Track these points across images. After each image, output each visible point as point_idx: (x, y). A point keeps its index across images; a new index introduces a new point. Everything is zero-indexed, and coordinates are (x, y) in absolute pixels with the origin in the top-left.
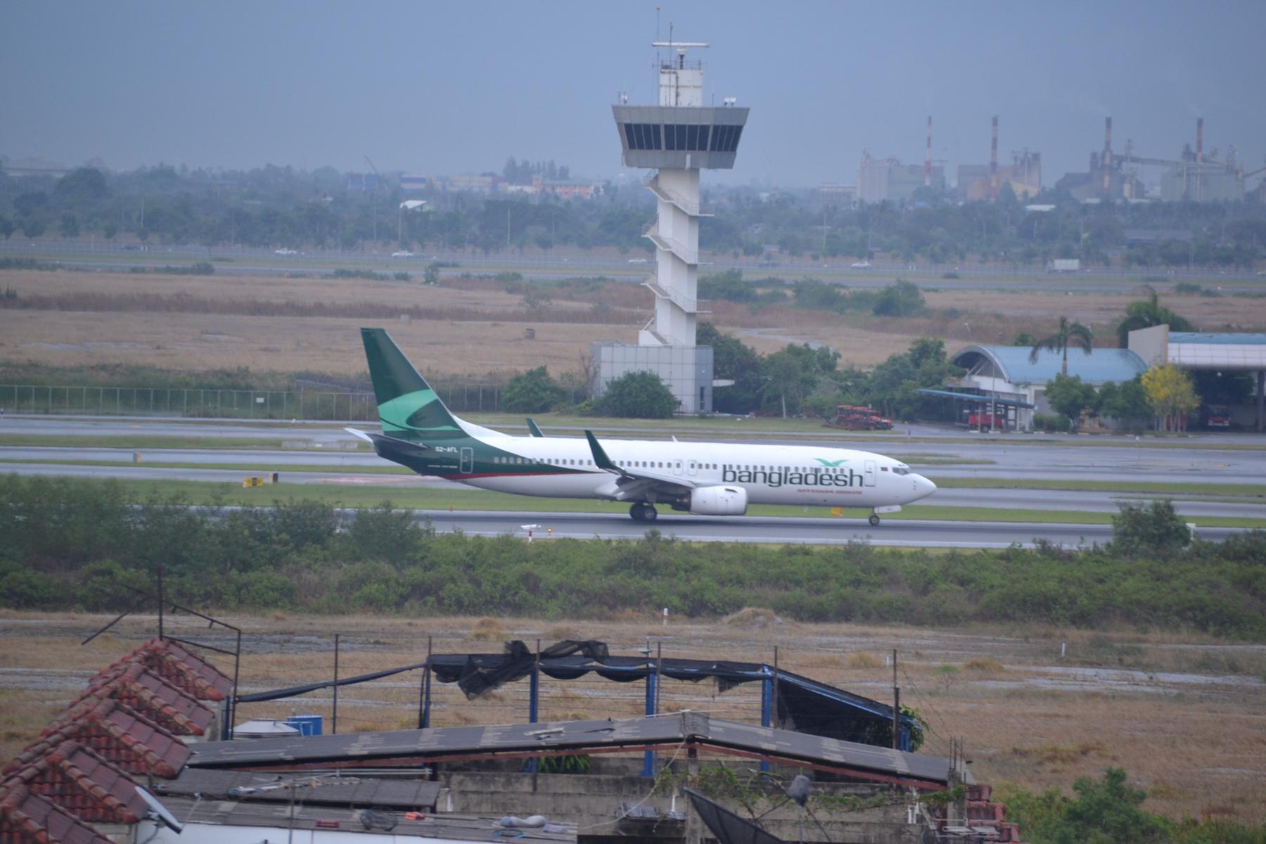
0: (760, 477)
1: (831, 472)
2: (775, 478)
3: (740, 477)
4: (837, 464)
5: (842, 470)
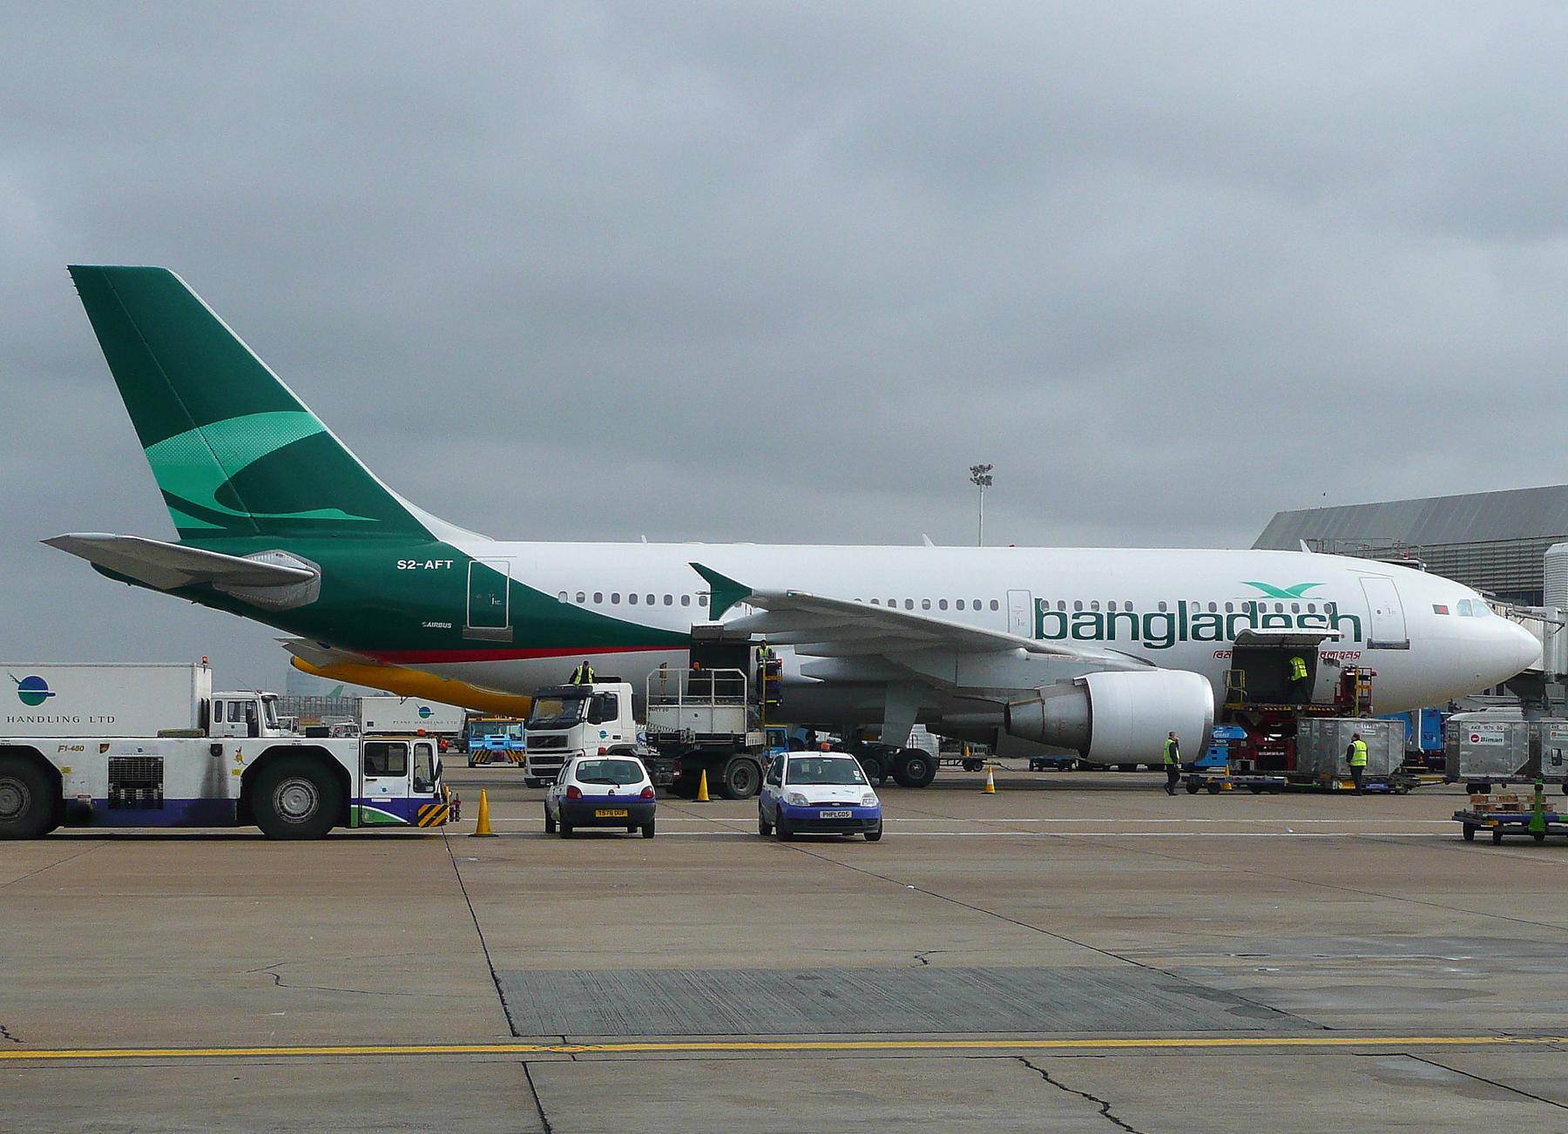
0: (1123, 625)
1: (1287, 611)
2: (1159, 627)
3: (1076, 628)
4: (1296, 591)
5: (1312, 607)
